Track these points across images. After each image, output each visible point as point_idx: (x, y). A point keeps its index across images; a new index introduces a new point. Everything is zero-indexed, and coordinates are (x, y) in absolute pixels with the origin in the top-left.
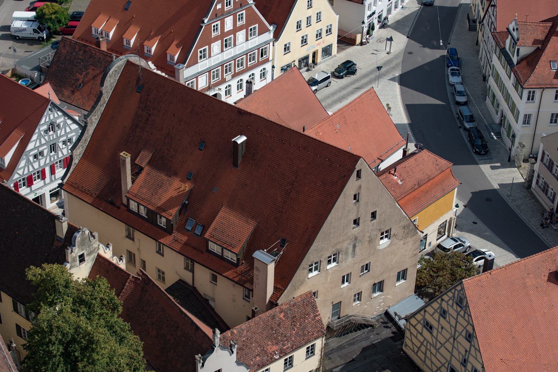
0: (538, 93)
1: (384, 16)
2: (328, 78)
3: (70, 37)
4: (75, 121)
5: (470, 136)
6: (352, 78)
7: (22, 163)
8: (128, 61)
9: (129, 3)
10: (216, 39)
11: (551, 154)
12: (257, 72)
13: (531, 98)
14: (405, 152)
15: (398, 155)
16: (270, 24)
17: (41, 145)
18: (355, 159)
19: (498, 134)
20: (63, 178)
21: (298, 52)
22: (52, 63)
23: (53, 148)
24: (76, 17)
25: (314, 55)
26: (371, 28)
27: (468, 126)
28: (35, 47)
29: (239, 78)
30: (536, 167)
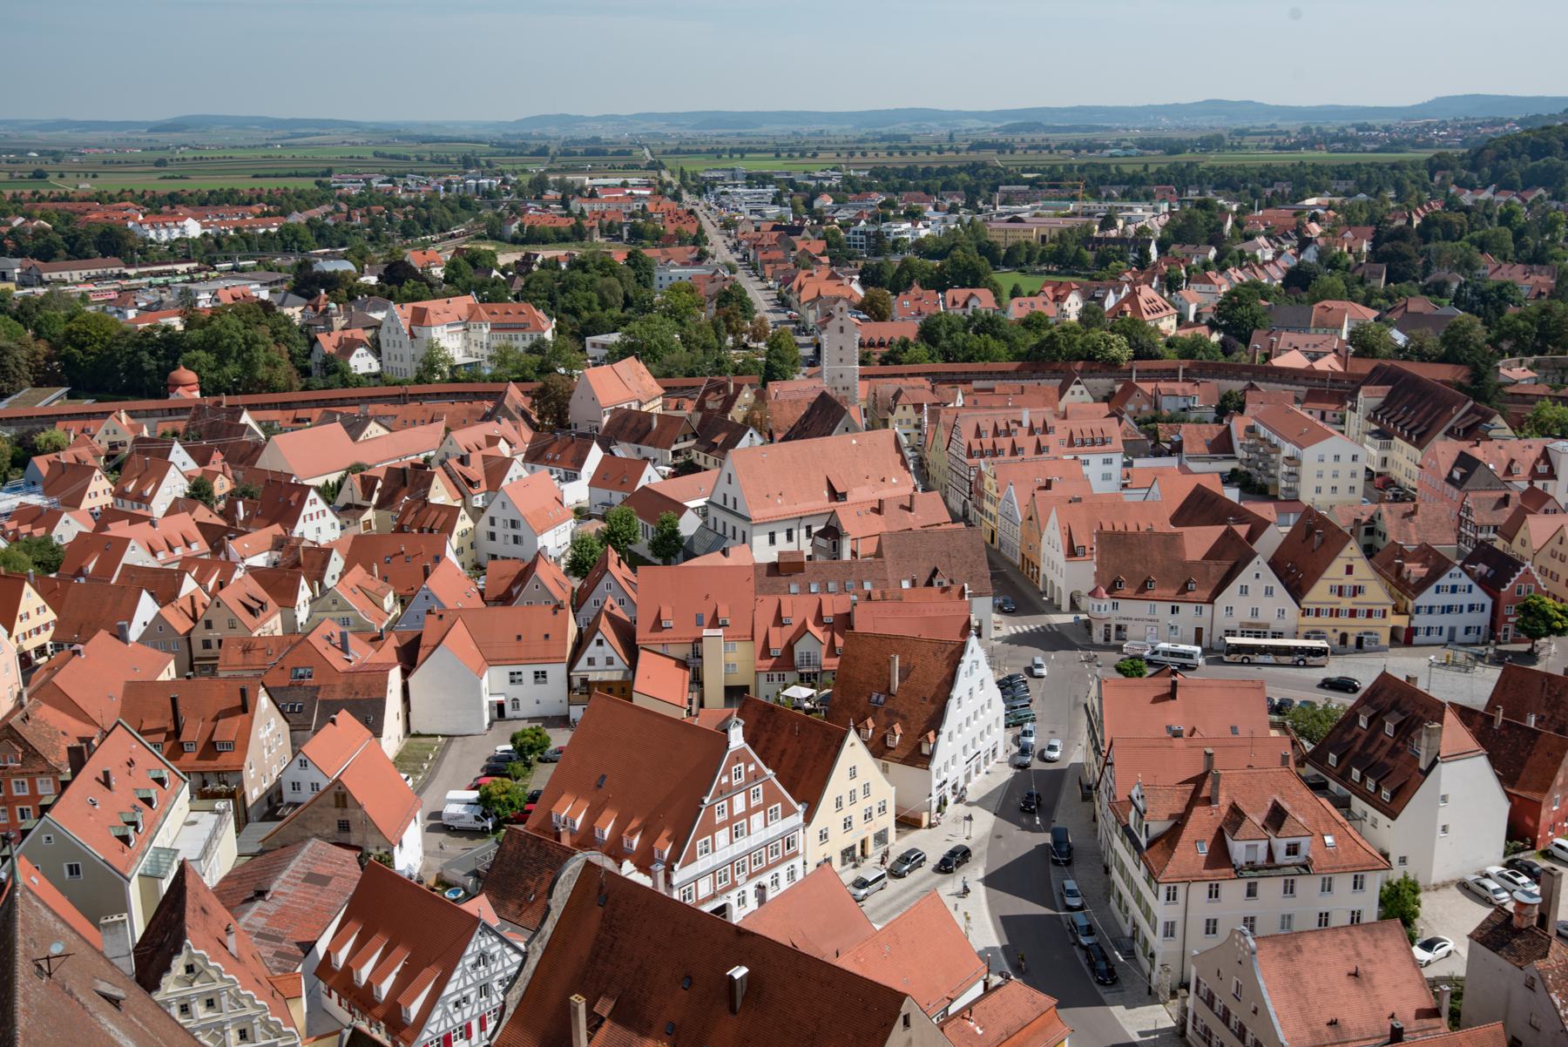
0: (1181, 889)
1: (960, 786)
2: (882, 877)
3: (520, 827)
4: (517, 950)
5: (1088, 957)
6: (918, 873)
7: (436, 1015)
8: (588, 862)
9: (603, 777)
10: (722, 826)
11: (1209, 983)
12: (782, 870)
13: (1171, 896)
14: (986, 985)
15: (978, 989)
16: (799, 802)
17: (467, 987)
18: (900, 997)
19: (1130, 954)
20: (490, 1039)
21: (841, 841)
22: (493, 864)
23: (484, 990)
24: (533, 798)
25: (863, 843)
26: (943, 802)
27: (1084, 941)
28: (478, 841)
29: (755, 881)
30: (1190, 1003)
